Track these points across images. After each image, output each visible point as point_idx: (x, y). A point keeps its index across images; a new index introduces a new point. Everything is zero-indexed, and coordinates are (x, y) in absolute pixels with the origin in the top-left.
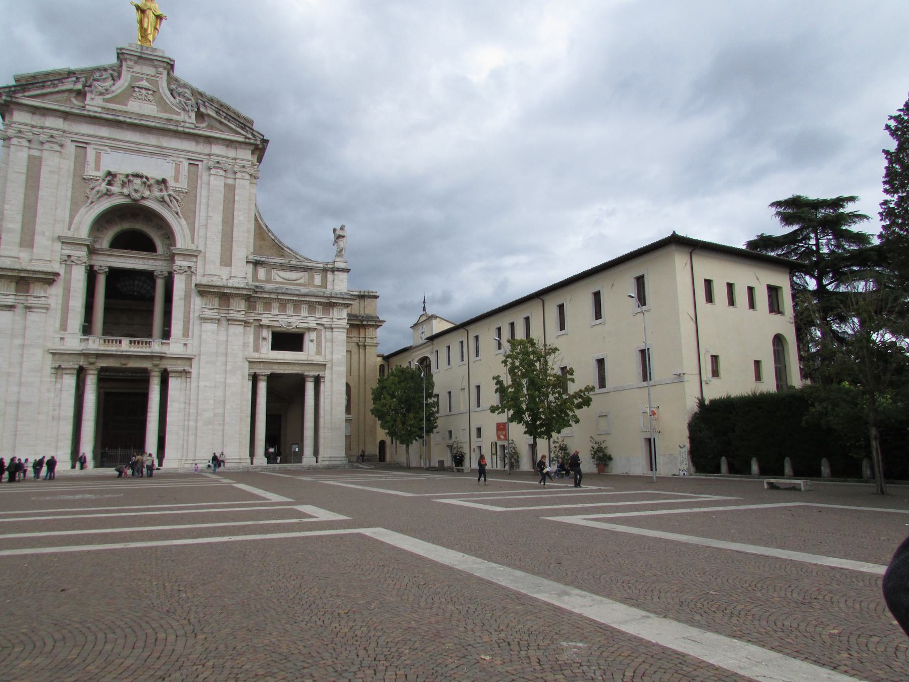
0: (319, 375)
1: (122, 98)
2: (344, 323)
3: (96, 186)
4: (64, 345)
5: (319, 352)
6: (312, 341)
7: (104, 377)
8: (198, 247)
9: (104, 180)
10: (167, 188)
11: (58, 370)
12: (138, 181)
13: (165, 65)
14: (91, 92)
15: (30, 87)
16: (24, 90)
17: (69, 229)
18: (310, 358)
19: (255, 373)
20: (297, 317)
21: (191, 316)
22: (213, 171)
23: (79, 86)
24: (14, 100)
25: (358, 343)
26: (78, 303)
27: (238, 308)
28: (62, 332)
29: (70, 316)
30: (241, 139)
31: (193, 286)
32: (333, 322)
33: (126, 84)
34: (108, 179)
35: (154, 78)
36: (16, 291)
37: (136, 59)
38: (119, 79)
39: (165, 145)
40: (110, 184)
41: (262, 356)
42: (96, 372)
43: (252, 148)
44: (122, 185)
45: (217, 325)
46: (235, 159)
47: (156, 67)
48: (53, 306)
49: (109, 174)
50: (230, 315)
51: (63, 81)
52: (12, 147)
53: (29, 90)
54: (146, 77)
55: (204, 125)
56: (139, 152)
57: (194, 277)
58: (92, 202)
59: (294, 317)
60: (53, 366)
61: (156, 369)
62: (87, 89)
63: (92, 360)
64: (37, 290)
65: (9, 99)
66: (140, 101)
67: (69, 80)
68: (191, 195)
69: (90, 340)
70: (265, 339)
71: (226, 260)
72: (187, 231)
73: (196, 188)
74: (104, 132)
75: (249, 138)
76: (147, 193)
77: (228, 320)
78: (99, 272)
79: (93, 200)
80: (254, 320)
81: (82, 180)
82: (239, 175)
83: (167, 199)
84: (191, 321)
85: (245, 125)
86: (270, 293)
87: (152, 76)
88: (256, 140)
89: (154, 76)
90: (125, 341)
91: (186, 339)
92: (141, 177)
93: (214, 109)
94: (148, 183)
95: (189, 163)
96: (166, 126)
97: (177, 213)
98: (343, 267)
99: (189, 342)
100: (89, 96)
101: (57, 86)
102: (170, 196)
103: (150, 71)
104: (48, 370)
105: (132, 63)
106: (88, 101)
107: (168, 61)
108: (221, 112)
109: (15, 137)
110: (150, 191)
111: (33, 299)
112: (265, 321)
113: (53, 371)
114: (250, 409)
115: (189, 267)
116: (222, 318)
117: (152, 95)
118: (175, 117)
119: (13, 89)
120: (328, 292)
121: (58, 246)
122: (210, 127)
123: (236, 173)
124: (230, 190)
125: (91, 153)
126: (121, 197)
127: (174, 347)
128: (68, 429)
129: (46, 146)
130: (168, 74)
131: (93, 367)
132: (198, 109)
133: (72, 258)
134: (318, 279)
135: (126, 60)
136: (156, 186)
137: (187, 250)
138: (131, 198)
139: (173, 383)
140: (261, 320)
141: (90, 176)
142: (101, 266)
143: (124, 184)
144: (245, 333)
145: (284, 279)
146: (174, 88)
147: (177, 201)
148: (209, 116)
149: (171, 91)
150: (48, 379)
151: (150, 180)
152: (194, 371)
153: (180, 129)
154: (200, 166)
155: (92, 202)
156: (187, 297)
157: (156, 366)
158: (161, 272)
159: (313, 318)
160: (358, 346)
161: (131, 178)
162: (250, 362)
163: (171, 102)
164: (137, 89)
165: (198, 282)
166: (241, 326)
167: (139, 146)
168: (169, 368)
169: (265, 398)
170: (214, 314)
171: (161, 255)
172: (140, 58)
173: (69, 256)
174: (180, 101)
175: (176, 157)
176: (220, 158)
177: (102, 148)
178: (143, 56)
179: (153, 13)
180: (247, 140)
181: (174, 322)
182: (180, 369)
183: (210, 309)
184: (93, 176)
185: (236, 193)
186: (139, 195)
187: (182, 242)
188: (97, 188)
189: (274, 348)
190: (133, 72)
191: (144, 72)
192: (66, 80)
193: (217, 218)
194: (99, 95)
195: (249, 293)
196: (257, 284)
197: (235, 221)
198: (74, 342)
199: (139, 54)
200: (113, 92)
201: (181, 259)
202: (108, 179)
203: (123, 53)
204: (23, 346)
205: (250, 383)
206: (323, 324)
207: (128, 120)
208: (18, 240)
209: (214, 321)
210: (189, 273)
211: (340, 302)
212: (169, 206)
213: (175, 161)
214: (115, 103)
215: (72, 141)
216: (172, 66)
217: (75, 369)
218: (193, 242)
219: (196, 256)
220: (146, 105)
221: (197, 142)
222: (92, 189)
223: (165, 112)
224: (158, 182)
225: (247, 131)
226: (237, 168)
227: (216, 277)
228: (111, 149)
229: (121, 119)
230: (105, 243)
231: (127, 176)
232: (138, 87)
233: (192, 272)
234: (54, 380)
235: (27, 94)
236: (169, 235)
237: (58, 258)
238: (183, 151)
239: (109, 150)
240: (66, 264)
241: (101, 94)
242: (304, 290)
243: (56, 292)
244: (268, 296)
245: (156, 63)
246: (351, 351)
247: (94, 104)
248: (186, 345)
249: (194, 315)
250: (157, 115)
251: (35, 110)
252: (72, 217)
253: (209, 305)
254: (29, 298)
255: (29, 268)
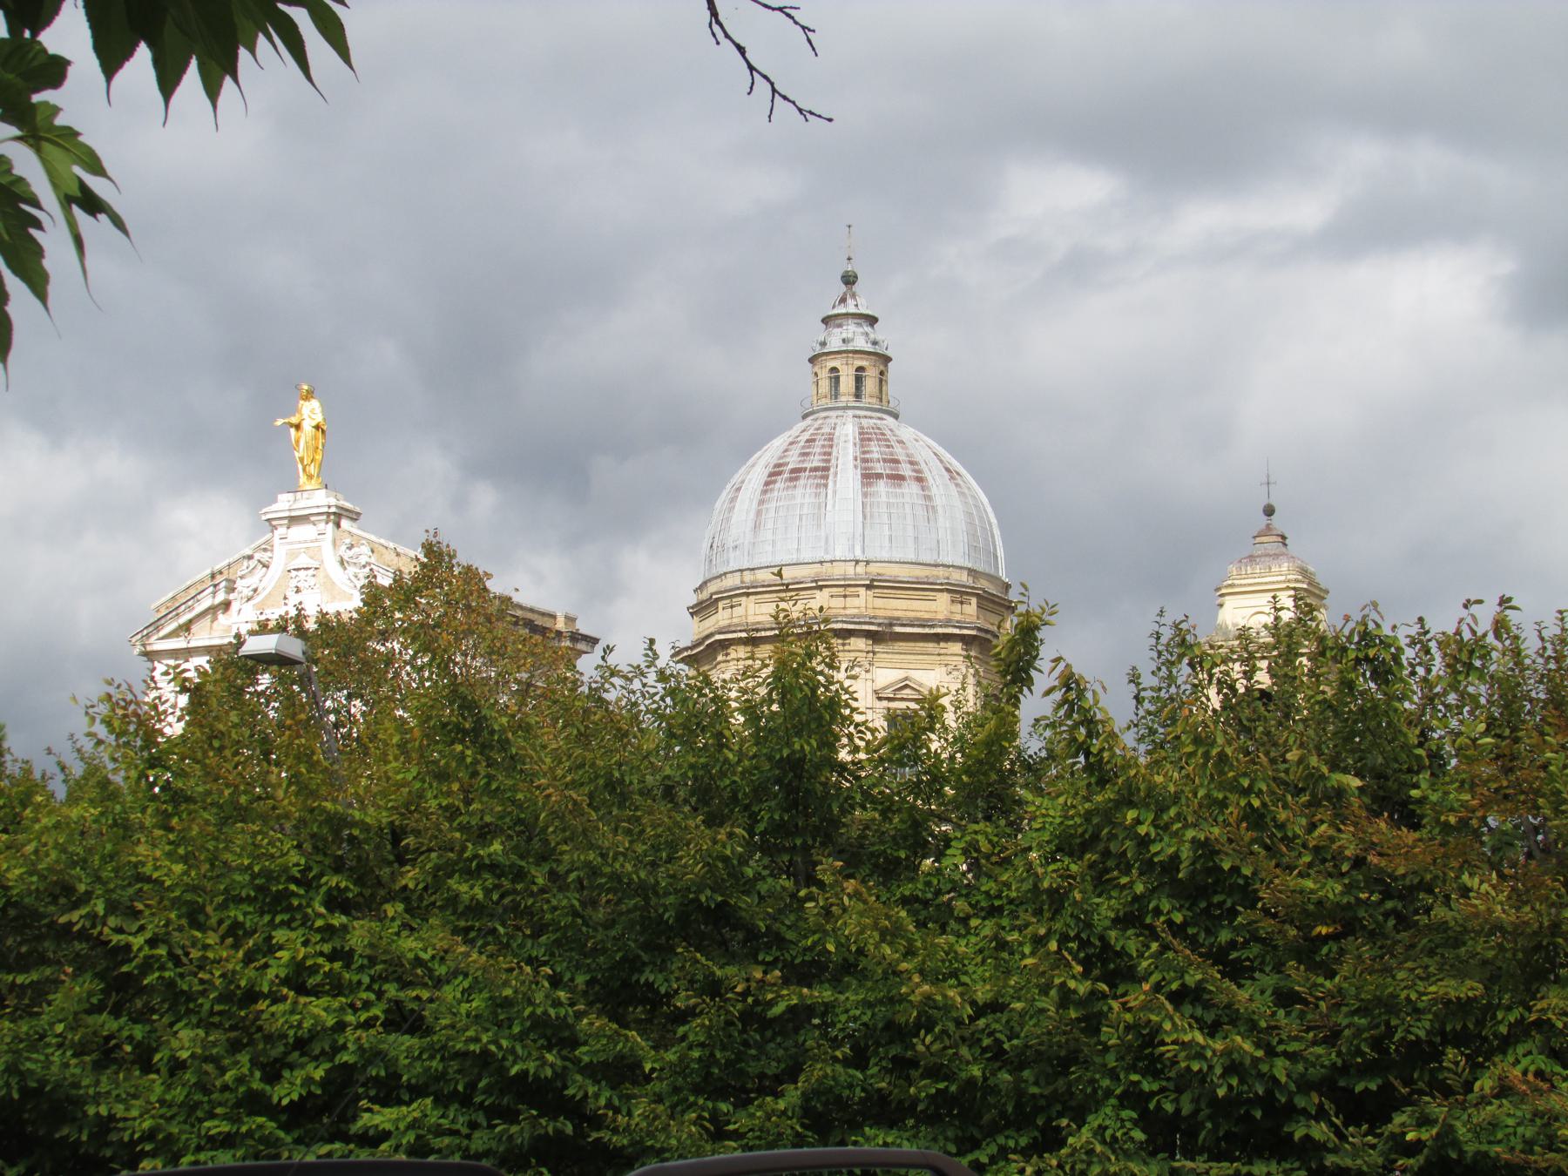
13: (324, 517)
15: (163, 621)
16: (158, 629)
23: (221, 597)
35: (316, 544)
37: (286, 522)
51: (199, 597)
89: (316, 540)
100: (235, 607)
164: (294, 573)
235: (162, 634)
245: (313, 519)
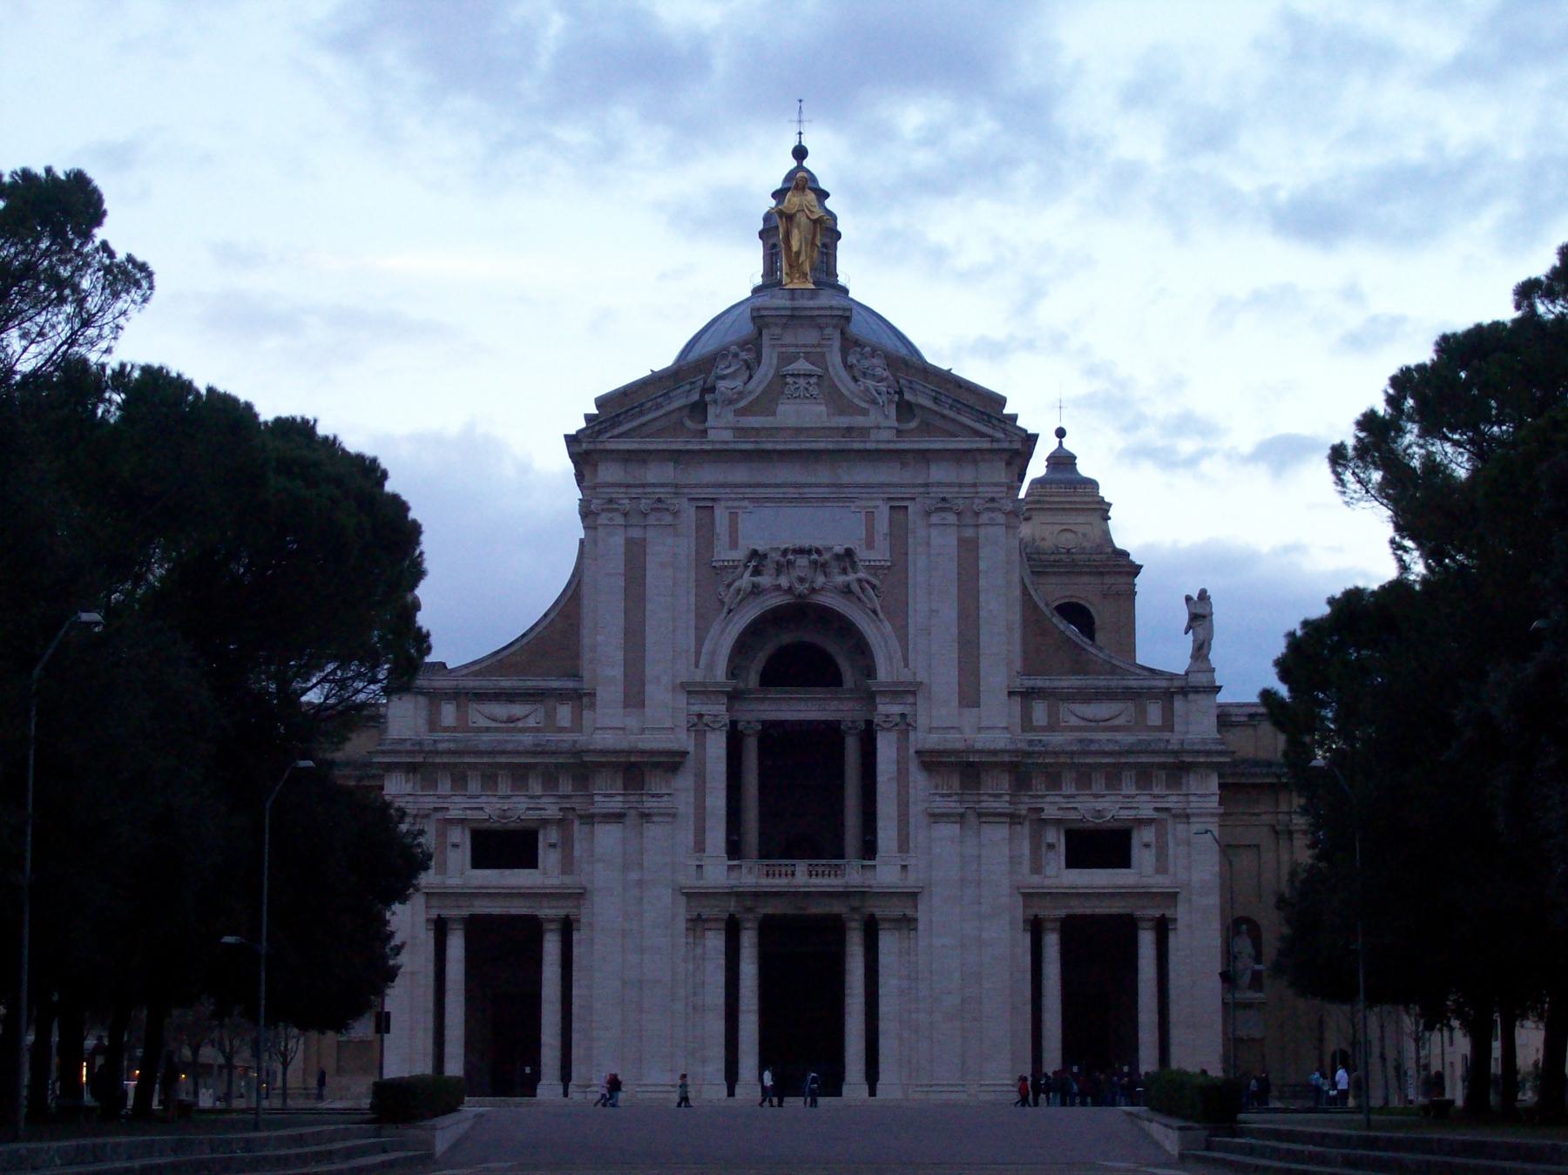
0: (1163, 915)
1: (766, 402)
2: (1213, 803)
3: (734, 581)
4: (702, 878)
5: (1161, 868)
6: (1147, 846)
7: (768, 928)
8: (915, 674)
9: (746, 567)
10: (854, 564)
11: (697, 924)
12: (802, 561)
14: (715, 402)
16: (613, 426)
17: (697, 666)
18: (1145, 881)
19: (1036, 916)
20: (1113, 798)
21: (912, 810)
22: (935, 519)
24: (600, 447)
25: (1273, 827)
26: (717, 801)
27: (997, 793)
28: (697, 854)
29: (708, 824)
30: (985, 444)
31: (912, 751)
32: (1189, 802)
33: (772, 372)
34: (753, 563)
35: (819, 350)
36: (625, 788)
37: (784, 321)
38: (759, 363)
39: (845, 479)
40: (757, 572)
41: (1047, 882)
42: (755, 925)
43: (1006, 456)
44: (777, 570)
45: (958, 826)
46: (974, 485)
47: (821, 329)
48: (682, 809)
49: (755, 553)
50: (983, 805)
52: (600, 529)
53: (620, 424)
54: (803, 350)
55: (913, 425)
56: (802, 500)
57: (912, 735)
58: (730, 611)
59: (1107, 799)
60: (689, 917)
61: (857, 917)
62: (708, 398)
63: (748, 903)
64: (655, 784)
65: (591, 447)
66: (798, 401)
67: (679, 391)
68: (895, 571)
69: (743, 867)
70: (1051, 846)
71: (969, 696)
72: (894, 644)
73: (906, 554)
74: (740, 474)
75: (998, 441)
76: (820, 580)
77: (980, 815)
78: (746, 732)
79: (732, 608)
80: (1030, 809)
81: (711, 572)
82: (984, 518)
83: (855, 587)
84: (912, 820)
85: (989, 416)
86: (1056, 754)
87: (813, 346)
88: (1011, 442)
89: (819, 345)
90: (801, 867)
91: (904, 855)
92: (809, 552)
93: (930, 393)
94: (821, 559)
95: (891, 507)
96: (842, 446)
97: (874, 612)
98: (1206, 685)
99: (911, 862)
100: (711, 410)
101: (662, 407)
102: (860, 581)
103: (809, 337)
104: (681, 925)
105: (777, 331)
106: (711, 421)
107: (840, 313)
108: (943, 398)
109: (603, 510)
110: (826, 576)
111: (650, 799)
112: (1051, 812)
113: (689, 925)
114: (1029, 986)
115: (903, 715)
116: (969, 811)
117: (817, 384)
118: (859, 421)
119: (597, 428)
120: (1174, 740)
121: (682, 699)
122: (926, 429)
123: (977, 514)
124: (969, 550)
125: (721, 516)
126: (778, 593)
127: (886, 874)
128: (718, 1026)
129: (651, 520)
130: (843, 333)
131: (751, 916)
132: (900, 393)
133: (706, 719)
134: (1154, 713)
135: (767, 326)
136: (834, 564)
137: (894, 683)
138: (793, 594)
139: (888, 942)
140: (1042, 810)
141: (723, 561)
142: (749, 722)
143: (779, 572)
144: (1011, 840)
145: (1083, 719)
146: (855, 362)
147: (874, 587)
148: (921, 407)
149: (849, 367)
150: (684, 940)
151: (824, 552)
152: (922, 916)
153: (871, 446)
154: (910, 510)
155: (730, 611)
156: (902, 775)
157: (853, 909)
158: (853, 722)
159: (1148, 798)
160: (1277, 833)
161: (791, 557)
162: (1024, 894)
163: (852, 392)
164: (789, 380)
165: (920, 746)
166: (1005, 825)
167: (801, 491)
168: (878, 913)
169: (1058, 966)
170: (953, 805)
171: (851, 690)
172: (792, 317)
173: (700, 716)
174: (867, 389)
175: (866, 499)
176: (945, 489)
177: (736, 504)
178: (797, 313)
179: (808, 218)
180: (996, 446)
181: (880, 824)
182: (897, 912)
183: (942, 795)
184: (728, 561)
185: (981, 555)
186: (807, 585)
187: (885, 672)
188: (737, 584)
189: (1071, 864)
190: (782, 346)
191: (800, 343)
192: (675, 393)
193: (949, 612)
194: (729, 404)
195: (1014, 759)
196: (1031, 736)
197: (983, 614)
198: (717, 873)
199: (789, 313)
200: (750, 392)
201: (887, 700)
202: (753, 563)
203: (762, 316)
204: (640, 883)
205: (1026, 940)
206: (1167, 810)
207: (779, 447)
208: (620, 696)
209: (952, 819)
210: (904, 727)
211: (1201, 760)
212: (859, 599)
213: (865, 508)
214: (754, 414)
215: (690, 499)
216: (848, 319)
217: (722, 920)
218: (906, 666)
219: (914, 693)
220: (806, 407)
221: (901, 463)
222: (729, 586)
223: (841, 413)
224: (837, 557)
225: (994, 427)
226: (978, 504)
227: (952, 731)
228: (754, 502)
229: (769, 446)
230: (753, 679)
231: (785, 552)
232: (792, 375)
233: (909, 725)
234: (691, 940)
235: (616, 431)
236: (861, 649)
237: (684, 725)
238: (881, 485)
239: (750, 506)
240: (696, 731)
241: (731, 402)
242: (1127, 739)
243: (684, 782)
244: (1052, 761)
245: (819, 321)
246: (1257, 846)
247: (721, 427)
248: (904, 867)
249: (916, 810)
250: (828, 425)
251: (628, 457)
252: (700, 641)
253: (943, 789)
254: (644, 798)
255: (641, 746)
